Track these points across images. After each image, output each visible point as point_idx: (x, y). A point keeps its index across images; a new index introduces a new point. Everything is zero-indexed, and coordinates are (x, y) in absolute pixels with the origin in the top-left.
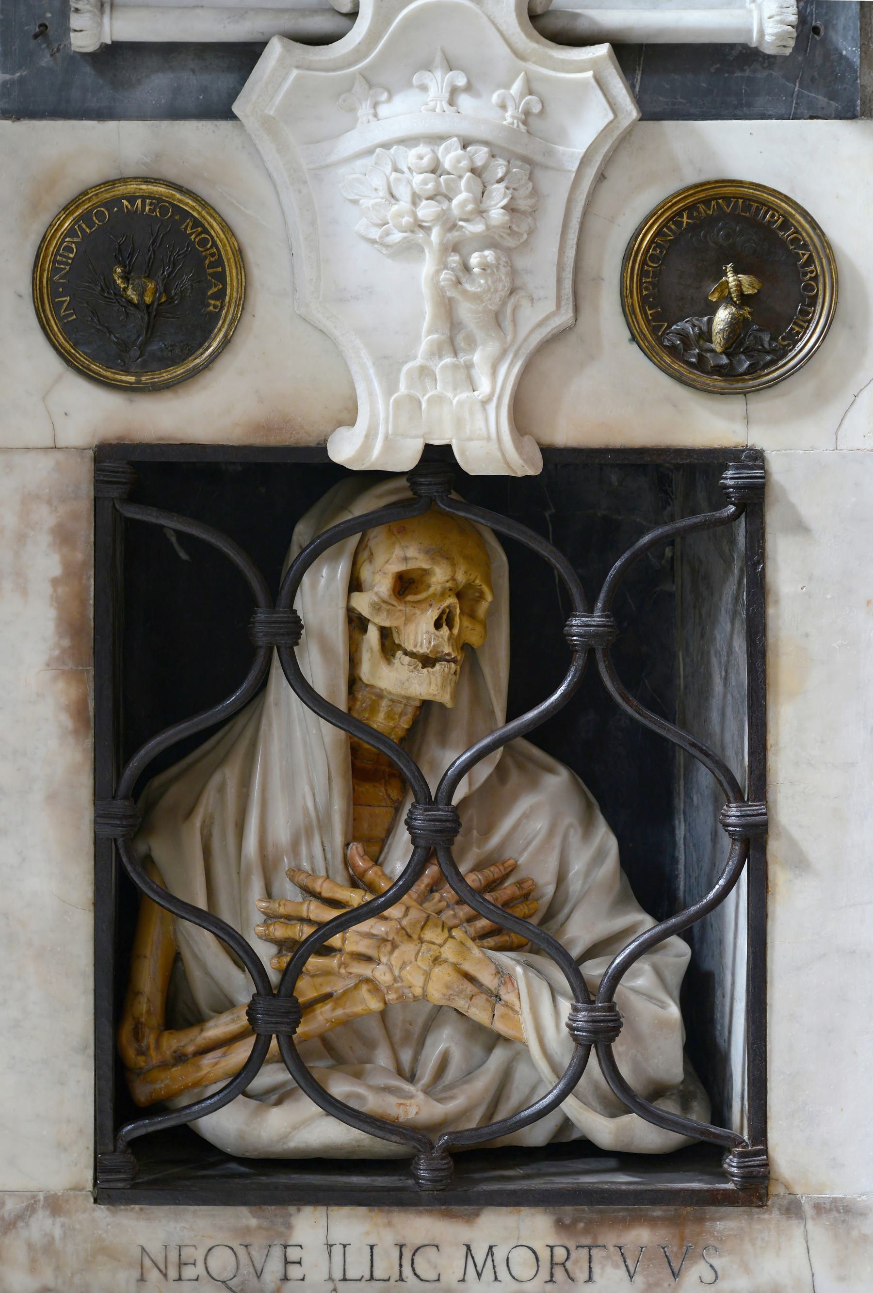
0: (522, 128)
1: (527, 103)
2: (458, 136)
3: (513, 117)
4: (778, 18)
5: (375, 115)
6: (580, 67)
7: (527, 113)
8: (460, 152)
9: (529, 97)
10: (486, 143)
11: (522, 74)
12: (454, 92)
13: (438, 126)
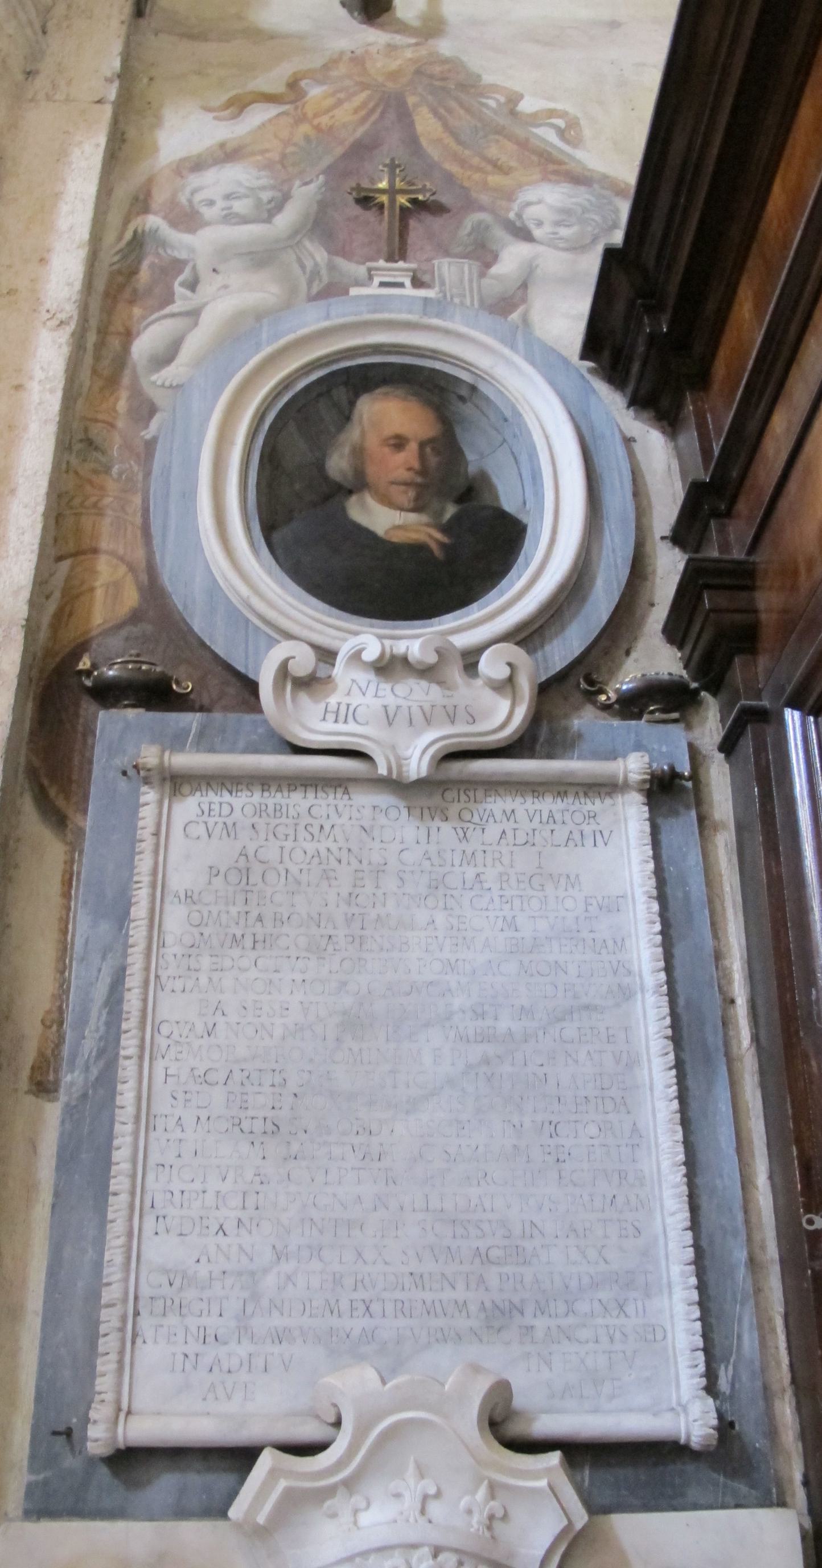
0: (487, 1534)
1: (490, 1509)
2: (429, 1545)
3: (479, 1523)
4: (700, 1422)
5: (355, 1523)
6: (536, 1475)
7: (491, 1517)
8: (431, 1562)
9: (492, 1503)
10: (457, 1551)
11: (486, 1482)
12: (425, 1498)
13: (412, 1537)
